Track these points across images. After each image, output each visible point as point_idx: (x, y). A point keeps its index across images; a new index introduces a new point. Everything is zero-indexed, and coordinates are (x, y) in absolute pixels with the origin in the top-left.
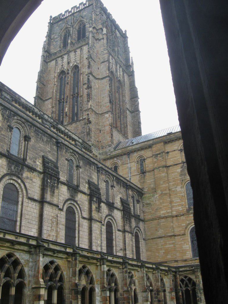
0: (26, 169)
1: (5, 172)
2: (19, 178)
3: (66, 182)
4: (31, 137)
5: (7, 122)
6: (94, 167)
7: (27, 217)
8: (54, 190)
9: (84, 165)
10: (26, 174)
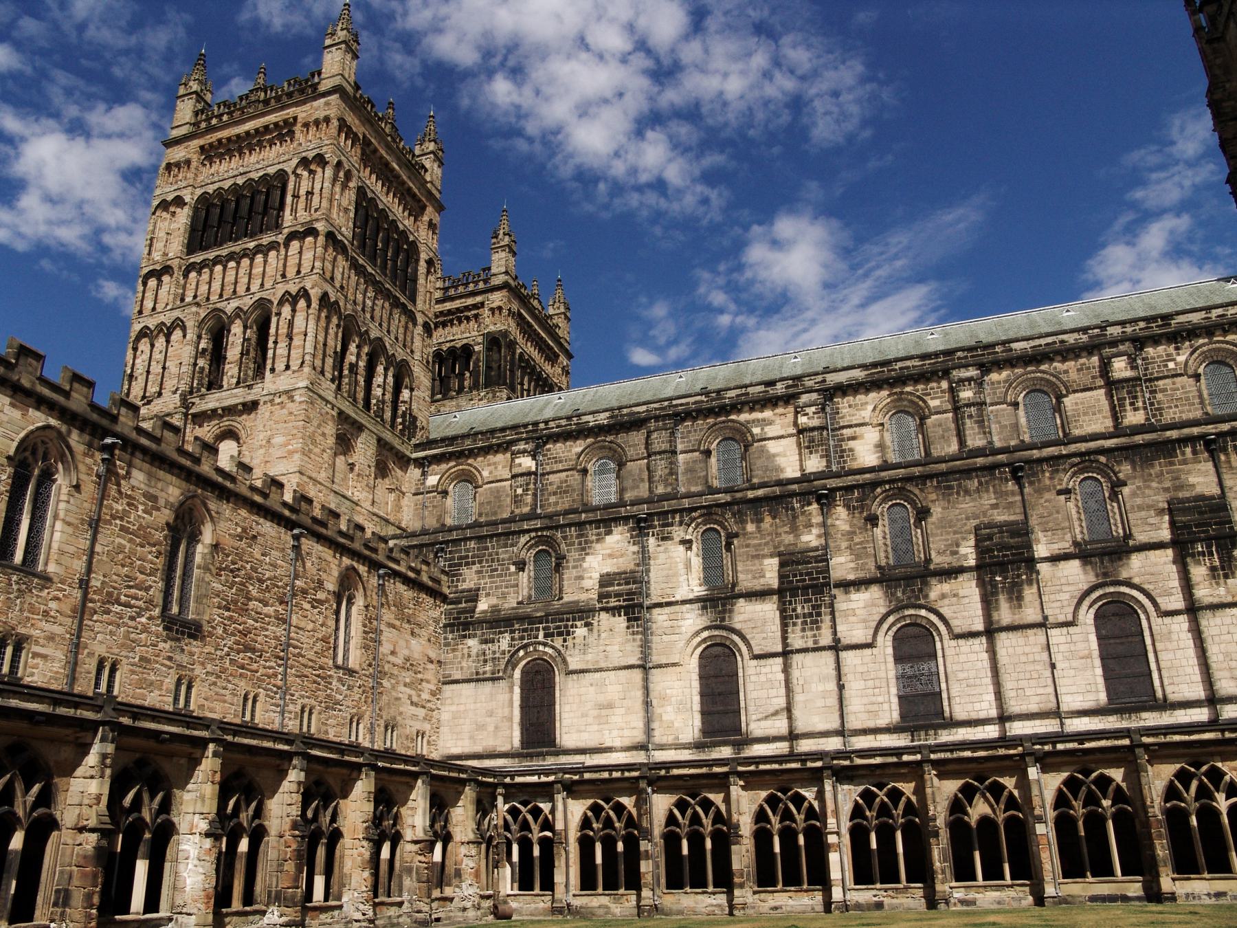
0: (933, 581)
1: (883, 610)
2: (920, 607)
3: (1072, 549)
4: (930, 505)
5: (861, 512)
6: (1188, 450)
7: (961, 675)
8: (1020, 592)
9: (1142, 467)
10: (937, 589)
